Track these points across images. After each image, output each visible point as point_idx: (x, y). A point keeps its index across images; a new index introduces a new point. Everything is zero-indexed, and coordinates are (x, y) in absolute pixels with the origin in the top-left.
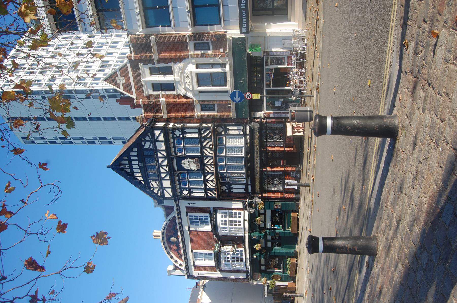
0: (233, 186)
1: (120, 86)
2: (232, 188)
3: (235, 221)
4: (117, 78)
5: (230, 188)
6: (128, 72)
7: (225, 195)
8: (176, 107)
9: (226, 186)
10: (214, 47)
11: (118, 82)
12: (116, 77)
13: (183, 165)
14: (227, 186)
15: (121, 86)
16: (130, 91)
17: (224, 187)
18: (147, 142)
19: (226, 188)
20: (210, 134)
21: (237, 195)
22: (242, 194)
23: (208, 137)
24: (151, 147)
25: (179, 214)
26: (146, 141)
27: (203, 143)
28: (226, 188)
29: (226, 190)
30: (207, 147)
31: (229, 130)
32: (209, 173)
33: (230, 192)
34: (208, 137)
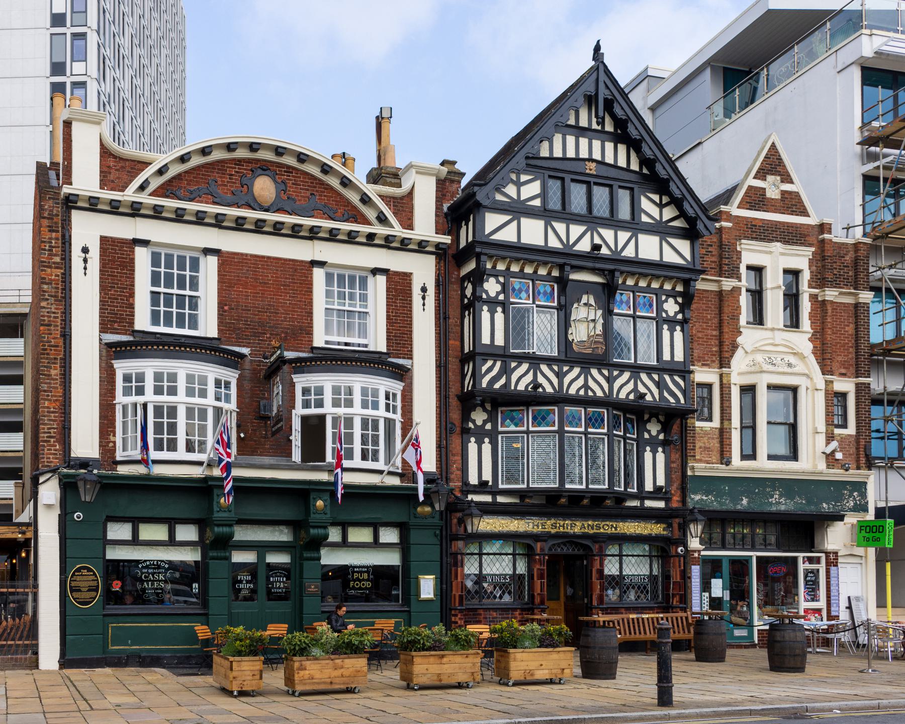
0: (487, 447)
1: (759, 179)
2: (480, 443)
3: (364, 441)
4: (778, 178)
5: (480, 435)
6: (792, 214)
7: (455, 415)
8: (709, 317)
9: (485, 422)
10: (842, 438)
11: (770, 178)
12: (782, 179)
13: (584, 299)
14: (488, 426)
15: (758, 183)
16: (747, 202)
17: (485, 416)
18: (657, 210)
19: (479, 422)
20: (672, 400)
21: (453, 455)
22: (459, 473)
23: (666, 394)
24: (645, 219)
25: (388, 243)
26: (661, 206)
27: (647, 373)
28: (479, 422)
29: (474, 422)
30: (636, 385)
31: (654, 452)
32: (560, 375)
33: (466, 432)
34: (666, 394)
